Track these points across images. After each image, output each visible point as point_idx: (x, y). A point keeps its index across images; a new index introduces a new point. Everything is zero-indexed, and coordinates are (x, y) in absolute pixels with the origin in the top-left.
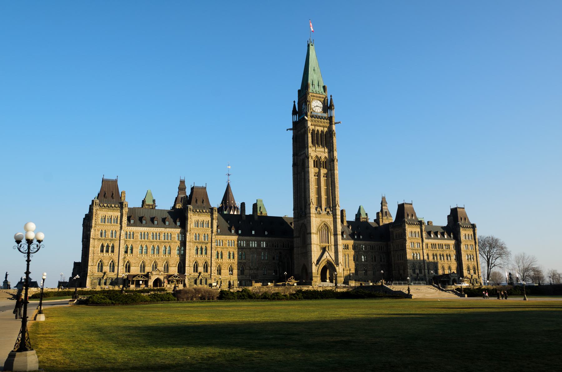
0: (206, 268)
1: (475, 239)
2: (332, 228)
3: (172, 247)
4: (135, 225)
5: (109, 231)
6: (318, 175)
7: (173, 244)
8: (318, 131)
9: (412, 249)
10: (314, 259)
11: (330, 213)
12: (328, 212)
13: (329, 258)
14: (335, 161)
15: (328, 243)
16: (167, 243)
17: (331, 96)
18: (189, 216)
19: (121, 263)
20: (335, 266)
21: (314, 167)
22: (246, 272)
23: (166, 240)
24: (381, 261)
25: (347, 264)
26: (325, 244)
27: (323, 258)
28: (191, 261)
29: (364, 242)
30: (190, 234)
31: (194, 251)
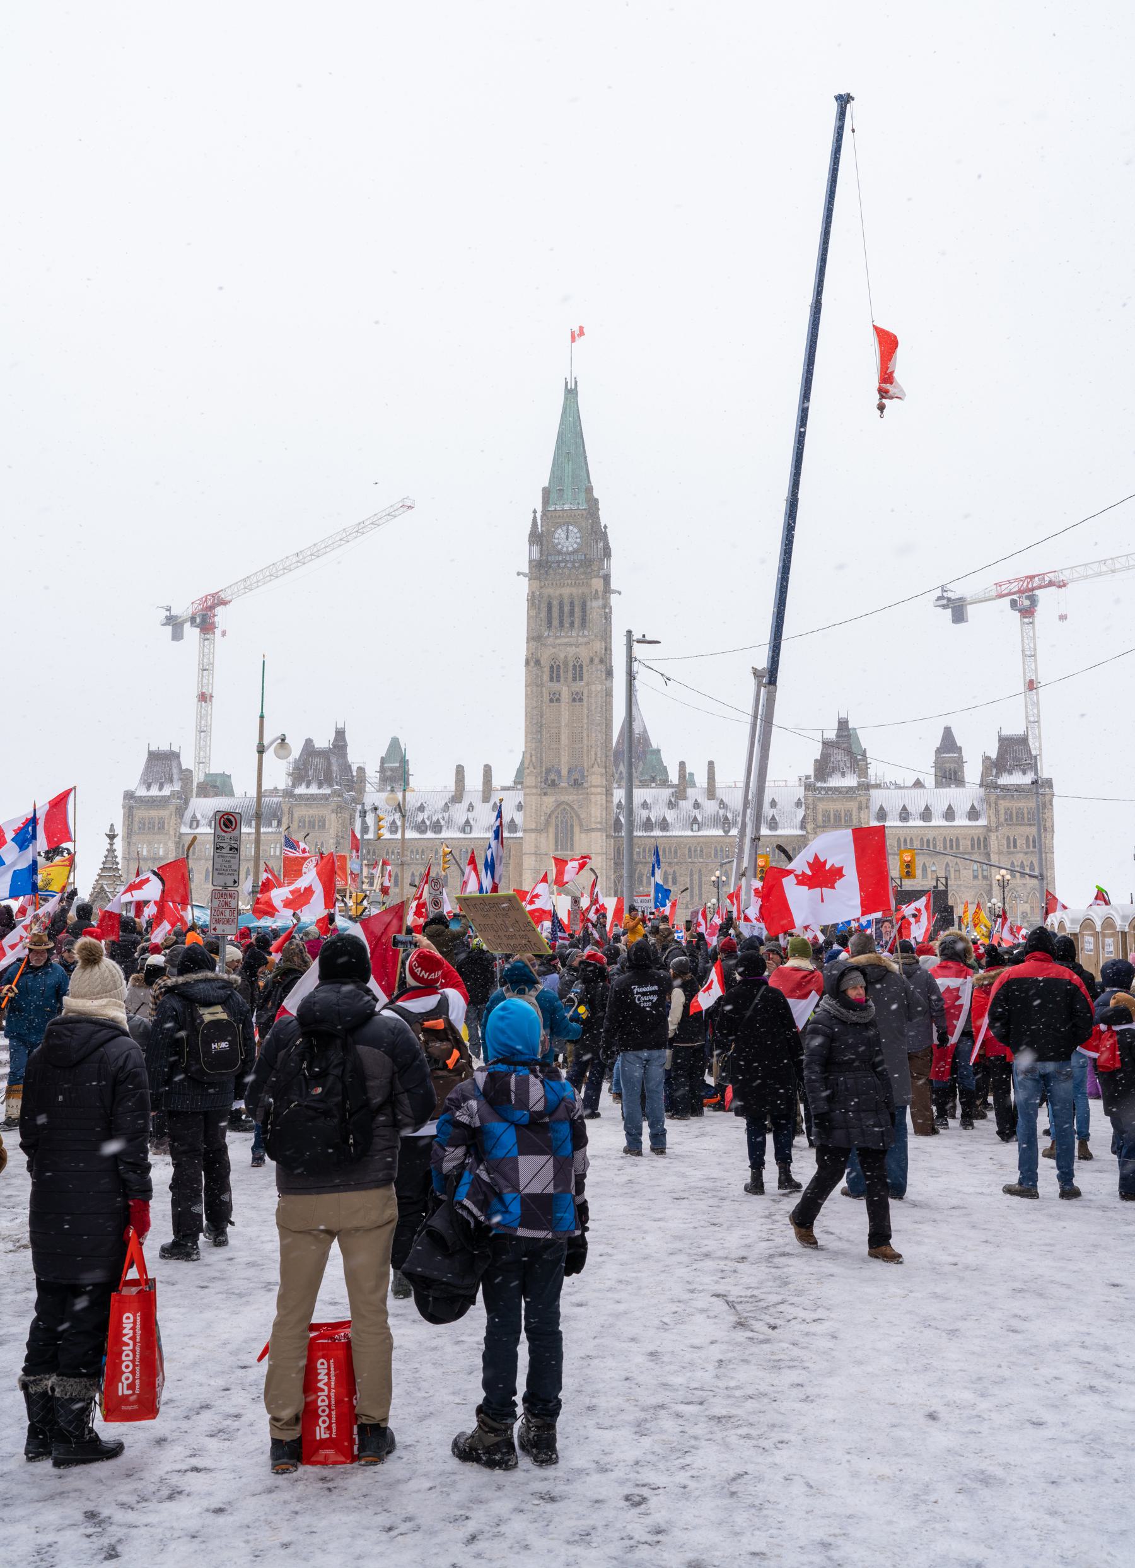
8: (561, 595)
14: (596, 661)
21: (551, 680)
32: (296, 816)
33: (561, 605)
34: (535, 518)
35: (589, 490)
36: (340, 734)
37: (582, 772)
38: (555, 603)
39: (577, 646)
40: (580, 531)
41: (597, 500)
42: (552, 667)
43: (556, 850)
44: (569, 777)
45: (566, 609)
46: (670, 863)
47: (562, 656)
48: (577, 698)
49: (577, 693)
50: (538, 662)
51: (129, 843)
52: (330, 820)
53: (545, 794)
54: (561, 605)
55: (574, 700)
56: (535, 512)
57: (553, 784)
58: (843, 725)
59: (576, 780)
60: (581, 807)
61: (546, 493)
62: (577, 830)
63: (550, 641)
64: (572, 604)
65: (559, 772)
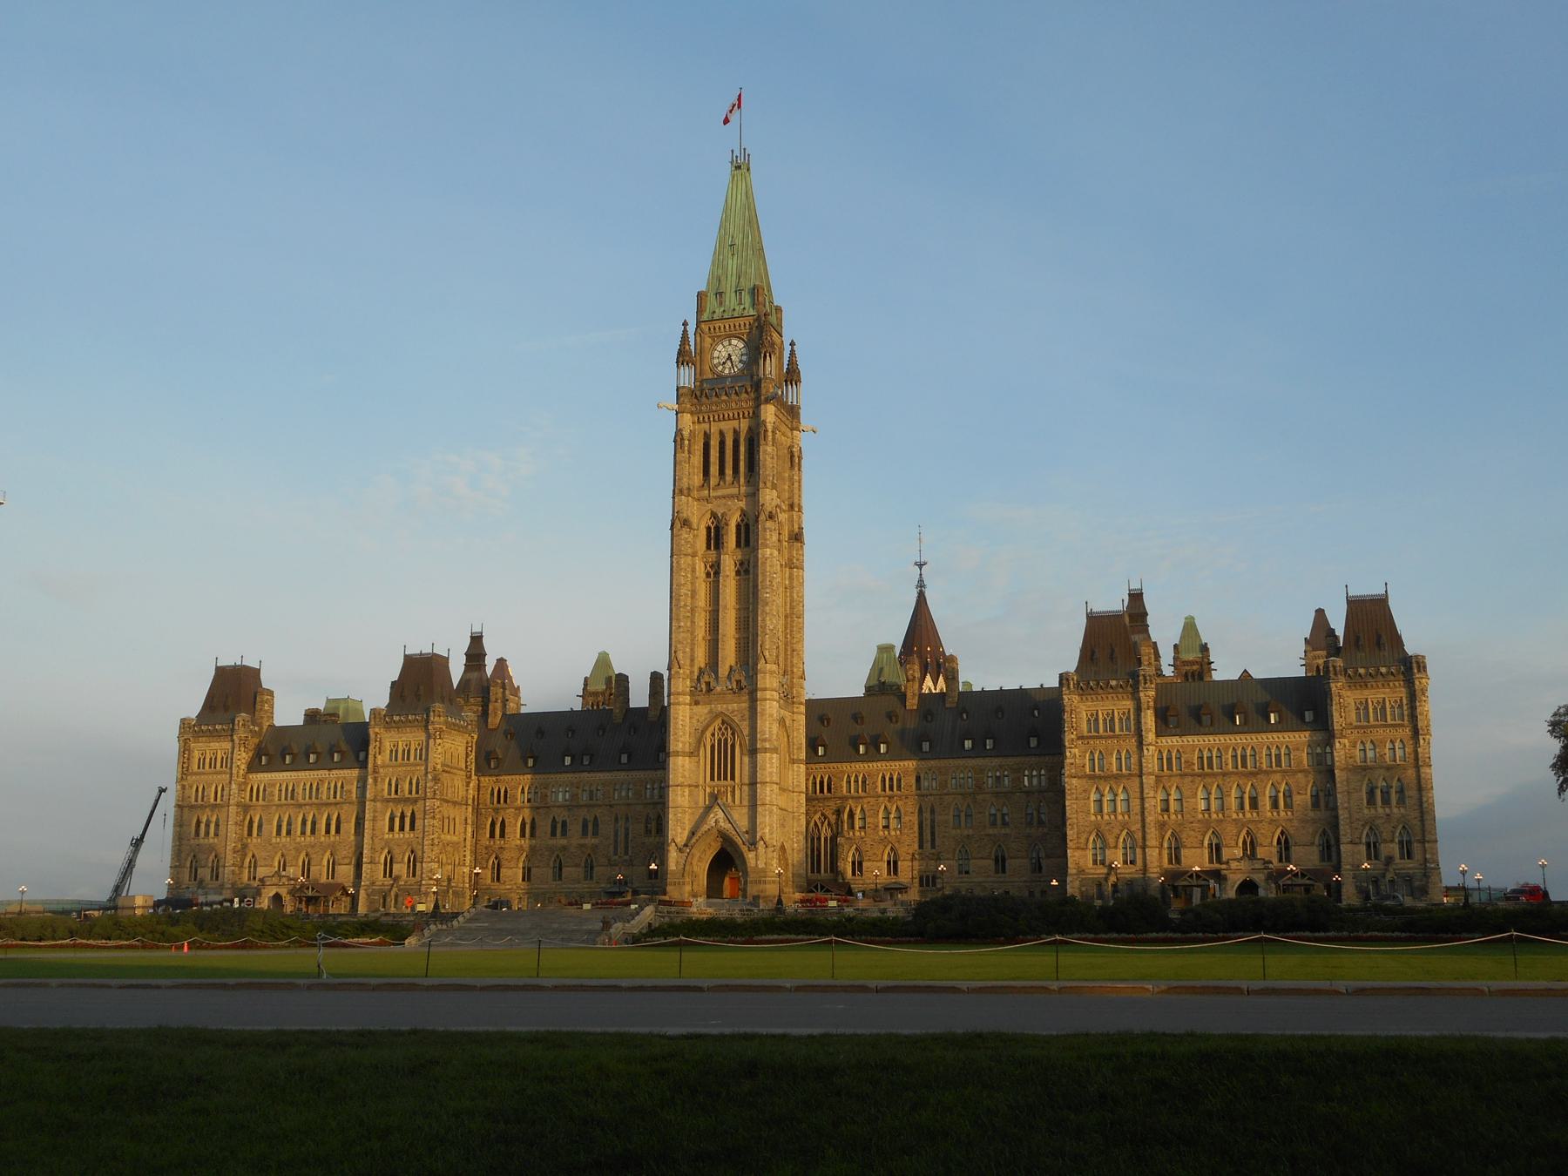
0: (414, 863)
1: (1413, 717)
2: (746, 732)
3: (343, 818)
4: (269, 769)
5: (210, 786)
6: (715, 571)
7: (345, 807)
8: (722, 433)
9: (1092, 777)
10: (678, 830)
11: (744, 683)
13: (724, 825)
14: (762, 517)
15: (733, 778)
18: (372, 736)
20: (744, 849)
21: (708, 547)
23: (332, 800)
26: (723, 782)
27: (705, 828)
28: (378, 848)
29: (996, 761)
30: (375, 780)
32: (387, 746)
33: (722, 444)
34: (685, 331)
36: (477, 640)
38: (715, 443)
41: (779, 310)
42: (709, 529)
43: (712, 779)
46: (890, 798)
50: (686, 523)
51: (183, 787)
53: (697, 703)
54: (722, 444)
55: (738, 573)
56: (685, 324)
57: (709, 690)
58: (1136, 598)
61: (701, 296)
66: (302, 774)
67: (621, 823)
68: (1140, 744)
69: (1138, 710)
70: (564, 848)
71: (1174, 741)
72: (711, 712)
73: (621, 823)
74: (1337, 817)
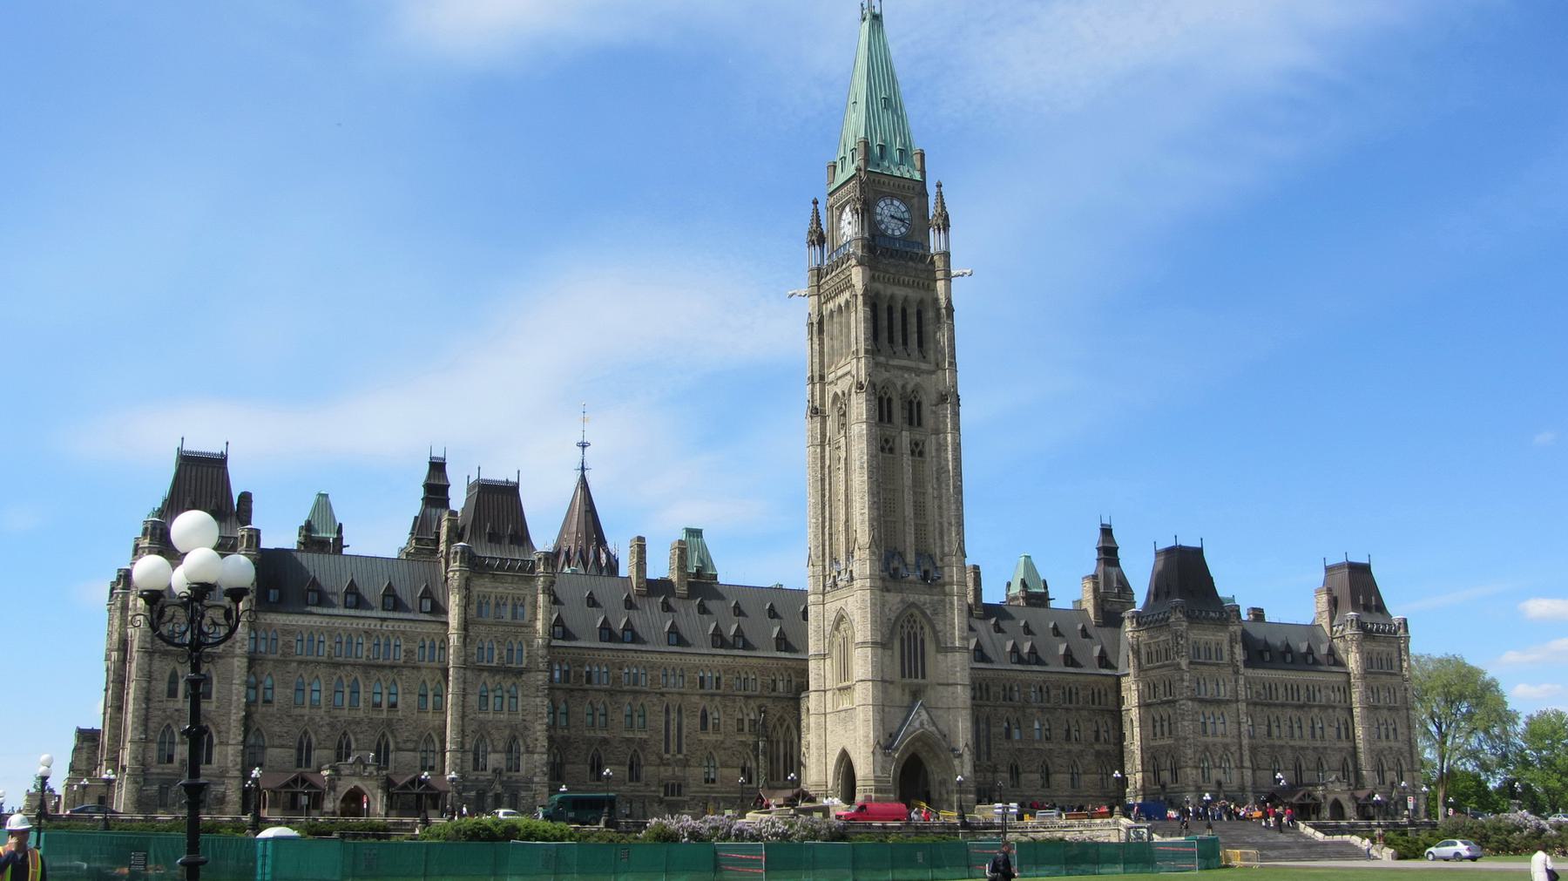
7: (405, 672)
8: (892, 297)
12: (926, 572)
15: (924, 677)
16: (387, 671)
17: (939, 186)
19: (236, 735)
22: (647, 771)
24: (1097, 739)
25: (984, 747)
31: (473, 699)
32: (474, 594)
33: (890, 309)
35: (922, 156)
37: (931, 557)
39: (919, 372)
40: (908, 210)
43: (903, 676)
44: (918, 567)
45: (897, 316)
47: (899, 384)
48: (917, 450)
49: (917, 445)
52: (535, 606)
53: (888, 591)
54: (890, 309)
55: (913, 452)
59: (926, 572)
60: (935, 612)
62: (930, 647)
63: (882, 359)
64: (904, 311)
65: (902, 555)
66: (338, 622)
67: (674, 715)
68: (1236, 672)
69: (1232, 641)
70: (605, 741)
71: (1250, 672)
72: (902, 601)
73: (674, 715)
74: (1355, 748)
